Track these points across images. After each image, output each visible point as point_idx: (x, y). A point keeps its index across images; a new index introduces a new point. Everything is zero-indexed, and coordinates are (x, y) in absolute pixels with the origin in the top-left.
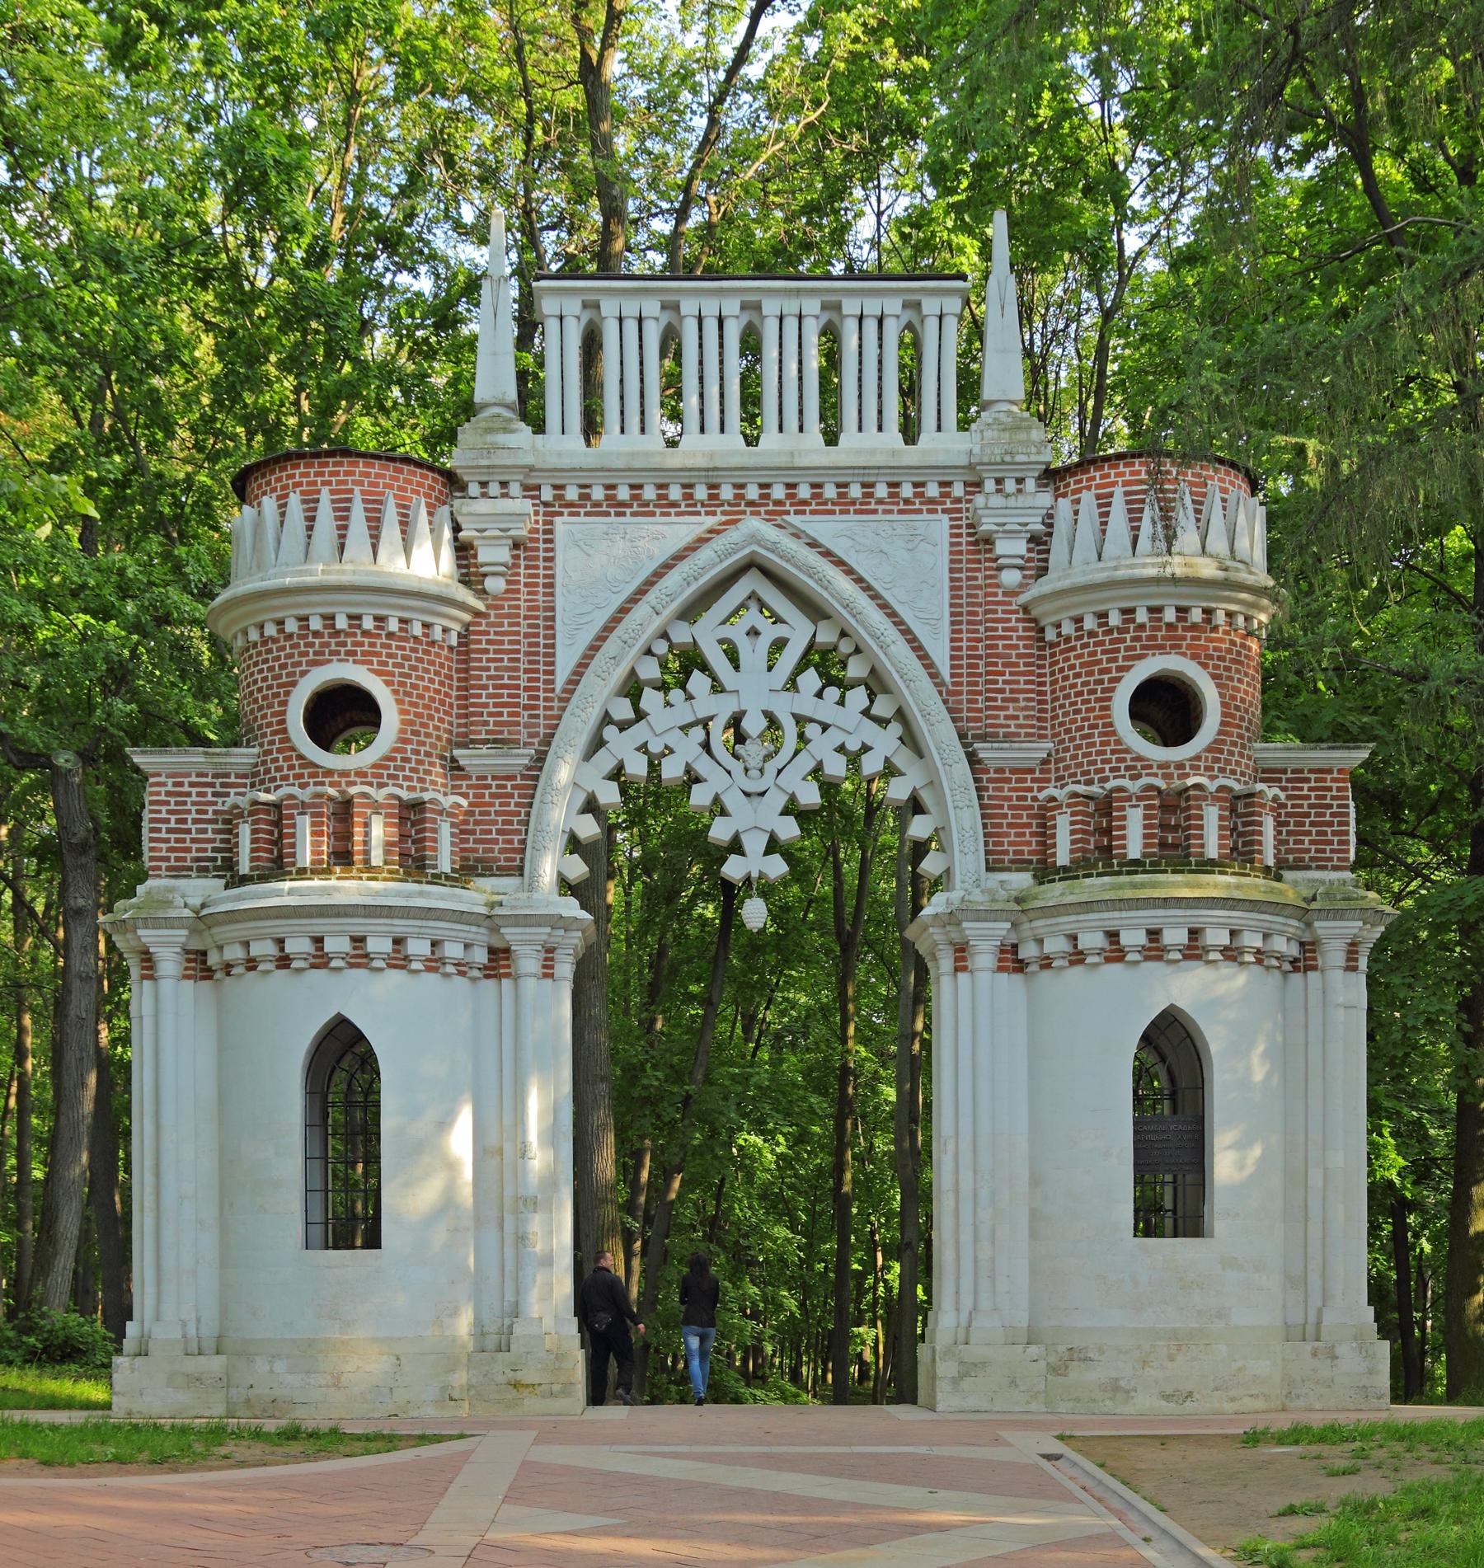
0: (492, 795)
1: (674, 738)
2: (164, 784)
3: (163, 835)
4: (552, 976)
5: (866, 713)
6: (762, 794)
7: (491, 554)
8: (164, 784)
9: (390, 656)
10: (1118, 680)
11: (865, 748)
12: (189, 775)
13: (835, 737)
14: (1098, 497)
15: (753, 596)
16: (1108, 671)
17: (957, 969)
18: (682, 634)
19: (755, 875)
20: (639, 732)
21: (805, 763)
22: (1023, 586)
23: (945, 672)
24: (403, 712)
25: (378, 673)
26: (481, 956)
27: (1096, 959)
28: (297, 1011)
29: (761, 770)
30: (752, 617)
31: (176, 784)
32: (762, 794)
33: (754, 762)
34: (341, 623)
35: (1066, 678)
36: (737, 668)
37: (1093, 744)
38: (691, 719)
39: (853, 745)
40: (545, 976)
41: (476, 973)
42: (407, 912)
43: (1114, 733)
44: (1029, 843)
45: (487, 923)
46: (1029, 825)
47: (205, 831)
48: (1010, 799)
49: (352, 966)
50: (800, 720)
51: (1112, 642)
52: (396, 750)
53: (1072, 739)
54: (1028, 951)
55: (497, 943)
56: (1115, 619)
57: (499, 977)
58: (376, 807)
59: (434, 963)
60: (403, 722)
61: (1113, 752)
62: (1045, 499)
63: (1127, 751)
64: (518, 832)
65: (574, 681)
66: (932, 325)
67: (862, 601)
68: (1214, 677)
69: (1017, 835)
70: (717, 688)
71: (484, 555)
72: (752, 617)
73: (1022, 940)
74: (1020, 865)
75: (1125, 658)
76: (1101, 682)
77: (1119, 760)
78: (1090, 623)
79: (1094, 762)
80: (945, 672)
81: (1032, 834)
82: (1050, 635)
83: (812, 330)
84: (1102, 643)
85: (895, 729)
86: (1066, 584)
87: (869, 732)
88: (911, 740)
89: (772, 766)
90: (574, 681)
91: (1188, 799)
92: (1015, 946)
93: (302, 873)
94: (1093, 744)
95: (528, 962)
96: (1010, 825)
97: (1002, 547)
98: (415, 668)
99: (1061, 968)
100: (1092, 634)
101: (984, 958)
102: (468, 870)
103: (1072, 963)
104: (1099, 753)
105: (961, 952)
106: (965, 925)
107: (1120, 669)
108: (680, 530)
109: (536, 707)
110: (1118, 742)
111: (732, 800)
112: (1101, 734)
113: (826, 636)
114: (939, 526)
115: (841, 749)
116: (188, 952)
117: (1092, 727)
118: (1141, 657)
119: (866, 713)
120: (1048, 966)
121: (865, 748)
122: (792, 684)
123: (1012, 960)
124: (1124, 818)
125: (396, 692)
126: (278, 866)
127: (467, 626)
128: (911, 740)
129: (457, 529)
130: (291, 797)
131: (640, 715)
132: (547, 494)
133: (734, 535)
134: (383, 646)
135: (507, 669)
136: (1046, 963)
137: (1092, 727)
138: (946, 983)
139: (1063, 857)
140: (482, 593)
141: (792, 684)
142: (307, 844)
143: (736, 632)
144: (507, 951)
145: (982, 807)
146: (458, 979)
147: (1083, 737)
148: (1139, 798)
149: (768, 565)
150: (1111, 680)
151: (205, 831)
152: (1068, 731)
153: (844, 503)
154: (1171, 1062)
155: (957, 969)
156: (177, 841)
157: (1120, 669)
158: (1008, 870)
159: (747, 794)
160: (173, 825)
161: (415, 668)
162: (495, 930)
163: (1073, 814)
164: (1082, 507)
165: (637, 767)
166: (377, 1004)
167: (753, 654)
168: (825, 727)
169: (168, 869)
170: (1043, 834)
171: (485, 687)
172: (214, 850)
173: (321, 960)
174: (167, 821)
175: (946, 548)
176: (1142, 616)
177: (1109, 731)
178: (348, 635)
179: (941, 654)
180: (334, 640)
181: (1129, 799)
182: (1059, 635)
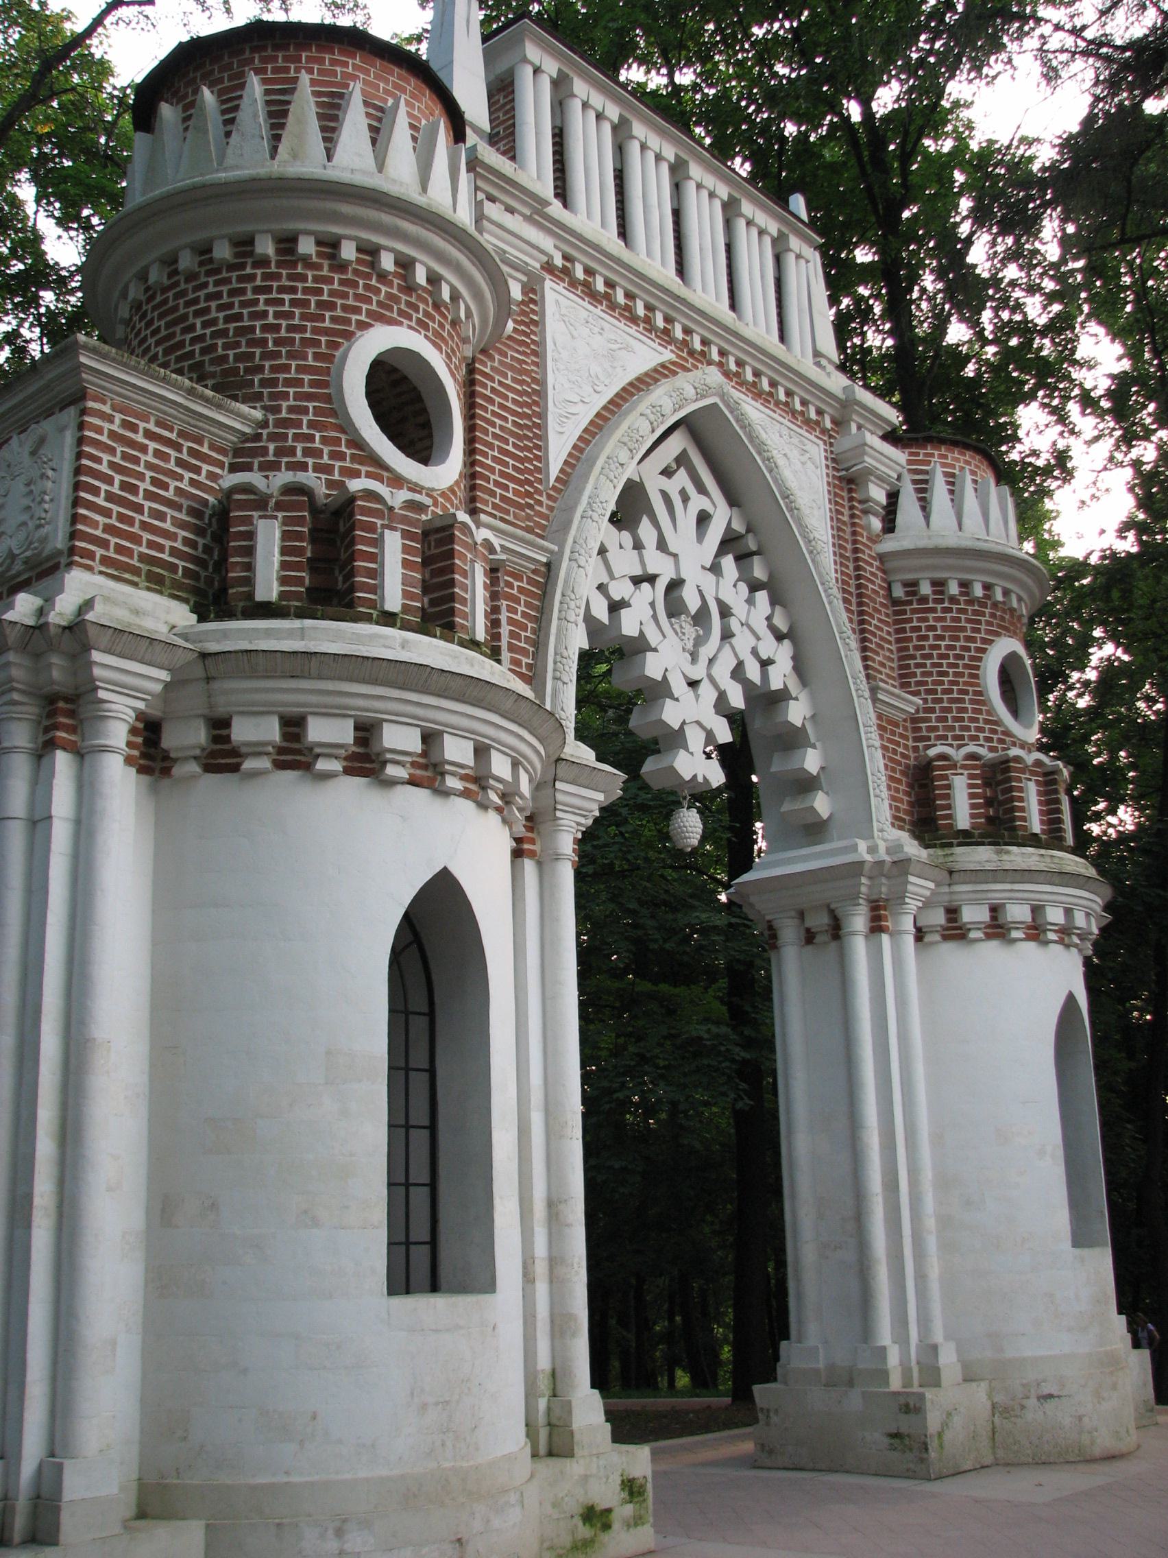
21: (726, 663)
37: (965, 710)
47: (161, 516)
70: (662, 545)
79: (968, 729)
87: (768, 647)
94: (965, 710)
103: (989, 937)
107: (984, 641)
110: (989, 713)
112: (972, 701)
113: (738, 527)
122: (715, 569)
141: (715, 569)
142: (394, 573)
151: (161, 516)
163: (971, 777)
167: (687, 521)
169: (105, 560)
172: (174, 552)
177: (980, 698)
181: (1023, 771)
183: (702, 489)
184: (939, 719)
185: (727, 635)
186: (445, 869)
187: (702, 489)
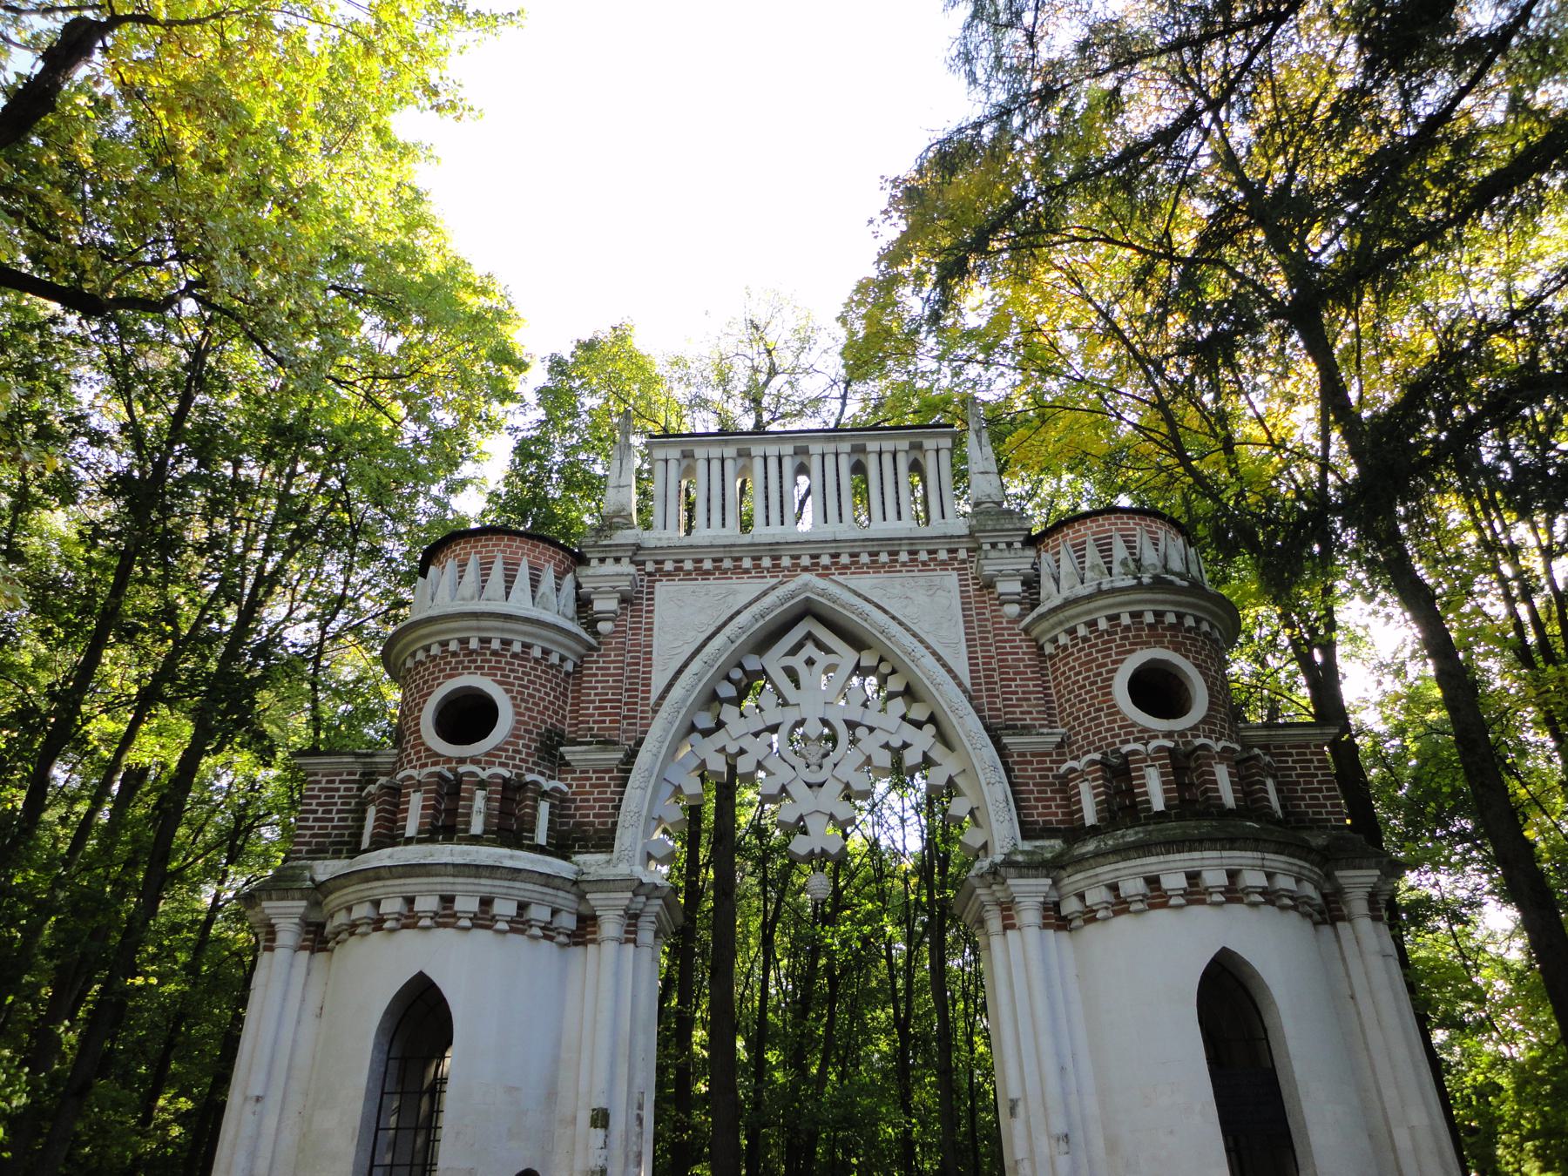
0: (592, 786)
1: (747, 742)
2: (319, 782)
3: (310, 823)
4: (634, 941)
5: (904, 718)
6: (821, 785)
7: (604, 604)
8: (319, 782)
9: (512, 671)
10: (1115, 670)
11: (906, 745)
12: (340, 774)
13: (881, 737)
14: (1073, 546)
15: (809, 636)
16: (1105, 665)
17: (1006, 928)
18: (752, 663)
19: (817, 850)
20: (720, 738)
22: (1022, 616)
23: (967, 683)
24: (518, 714)
25: (500, 683)
26: (568, 922)
27: (1141, 906)
28: (376, 970)
29: (821, 767)
30: (810, 650)
31: (328, 782)
32: (821, 785)
33: (813, 760)
34: (474, 644)
35: (1068, 678)
36: (798, 687)
37: (1102, 724)
38: (762, 727)
39: (896, 742)
40: (628, 941)
41: (562, 939)
42: (492, 870)
43: (1118, 712)
44: (1056, 814)
45: (574, 889)
46: (1054, 799)
48: (1033, 777)
49: (439, 925)
50: (851, 725)
51: (1104, 643)
52: (508, 743)
53: (1081, 724)
54: (1071, 906)
55: (584, 909)
56: (1103, 625)
57: (585, 944)
58: (482, 784)
59: (519, 924)
60: (518, 722)
61: (1121, 727)
62: (1031, 553)
63: (1133, 725)
64: (613, 815)
65: (662, 697)
66: (931, 456)
67: (894, 628)
68: (1197, 666)
69: (1044, 807)
71: (598, 605)
72: (810, 650)
73: (1061, 897)
74: (1048, 832)
75: (1117, 654)
76: (1100, 674)
77: (1127, 734)
78: (1082, 631)
80: (967, 683)
81: (1057, 807)
82: (1049, 649)
83: (845, 464)
84: (1096, 645)
85: (930, 729)
86: (1057, 601)
87: (909, 732)
88: (943, 737)
89: (828, 763)
90: (662, 697)
91: (1198, 757)
92: (1057, 905)
93: (409, 841)
94: (1102, 724)
95: (610, 926)
96: (1037, 800)
97: (1003, 587)
98: (534, 683)
99: (1105, 919)
100: (1085, 639)
101: (1029, 915)
102: (561, 846)
103: (1116, 913)
104: (1107, 730)
105: (1008, 910)
106: (1009, 882)
107: (1114, 662)
108: (747, 588)
109: (635, 717)
110: (1123, 719)
111: (798, 789)
114: (951, 579)
115: (886, 746)
116: (309, 924)
117: (1098, 710)
118: (1131, 651)
119: (904, 718)
120: (1094, 919)
121: (906, 745)
123: (1054, 918)
124: (1143, 777)
125: (514, 698)
126: (389, 836)
127: (581, 657)
128: (943, 737)
129: (578, 586)
130: (410, 777)
131: (720, 725)
132: (650, 567)
133: (792, 586)
134: (507, 663)
135: (611, 688)
136: (1090, 916)
137: (1098, 710)
138: (996, 942)
139: (1090, 818)
140: (596, 634)
143: (797, 661)
144: (594, 918)
145: (1012, 784)
146: (546, 943)
147: (1091, 720)
148: (1153, 760)
149: (823, 612)
150: (1108, 672)
152: (1076, 719)
153: (875, 566)
154: (1229, 1005)
155: (1006, 928)
156: (320, 828)
157: (1114, 662)
158: (1042, 838)
159: (810, 786)
160: (319, 815)
161: (534, 683)
162: (582, 897)
164: (1063, 556)
165: (718, 764)
166: (463, 966)
168: (871, 729)
170: (1067, 806)
171: (593, 702)
173: (409, 920)
174: (316, 812)
175: (958, 595)
176: (1126, 620)
177: (1114, 710)
178: (478, 654)
179: (963, 669)
180: (469, 657)
182: (1057, 648)
183: (828, 650)
184: (1084, 738)
185: (854, 742)
186: (421, 975)
187: (828, 650)
